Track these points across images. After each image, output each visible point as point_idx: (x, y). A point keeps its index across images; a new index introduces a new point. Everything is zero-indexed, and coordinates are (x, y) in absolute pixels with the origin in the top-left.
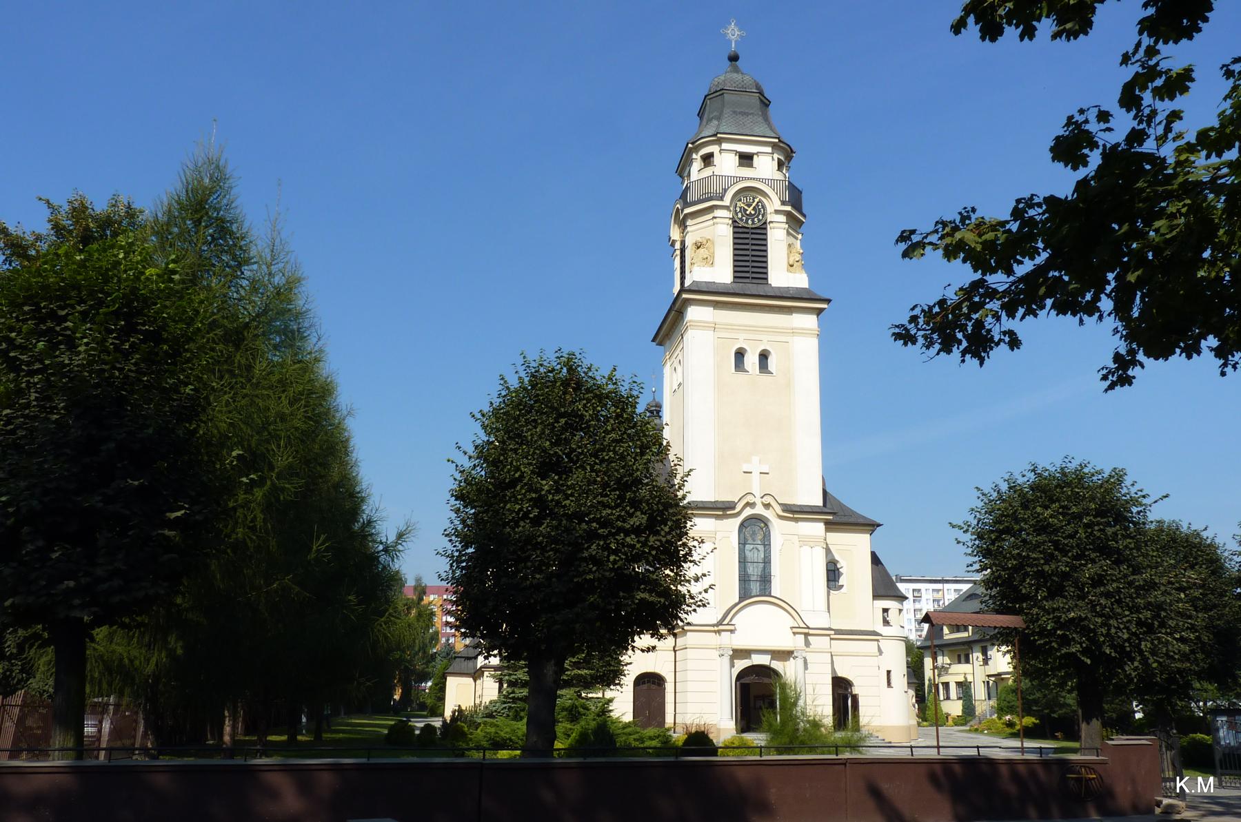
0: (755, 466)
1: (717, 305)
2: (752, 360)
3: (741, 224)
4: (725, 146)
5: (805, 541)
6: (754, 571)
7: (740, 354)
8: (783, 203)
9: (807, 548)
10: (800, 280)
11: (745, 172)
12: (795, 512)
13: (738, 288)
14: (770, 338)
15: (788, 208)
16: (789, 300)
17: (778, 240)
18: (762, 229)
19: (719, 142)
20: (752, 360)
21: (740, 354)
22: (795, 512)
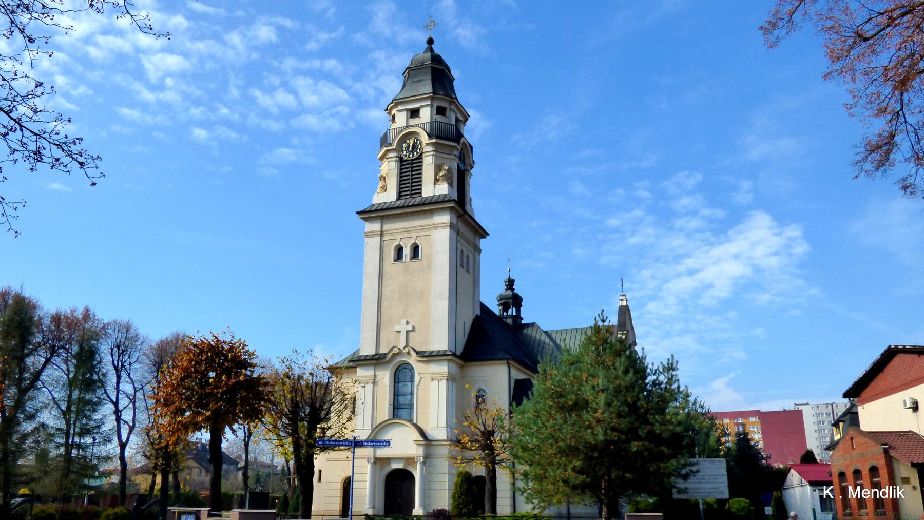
0: (404, 328)
1: (382, 218)
2: (407, 252)
3: (405, 158)
4: (400, 108)
5: (435, 378)
6: (402, 400)
7: (399, 250)
8: (430, 136)
9: (436, 382)
10: (443, 189)
11: (413, 121)
12: (428, 357)
13: (399, 203)
14: (419, 234)
15: (434, 141)
16: (433, 205)
17: (428, 163)
18: (420, 157)
19: (397, 105)
20: (407, 252)
21: (399, 250)
22: (428, 357)
